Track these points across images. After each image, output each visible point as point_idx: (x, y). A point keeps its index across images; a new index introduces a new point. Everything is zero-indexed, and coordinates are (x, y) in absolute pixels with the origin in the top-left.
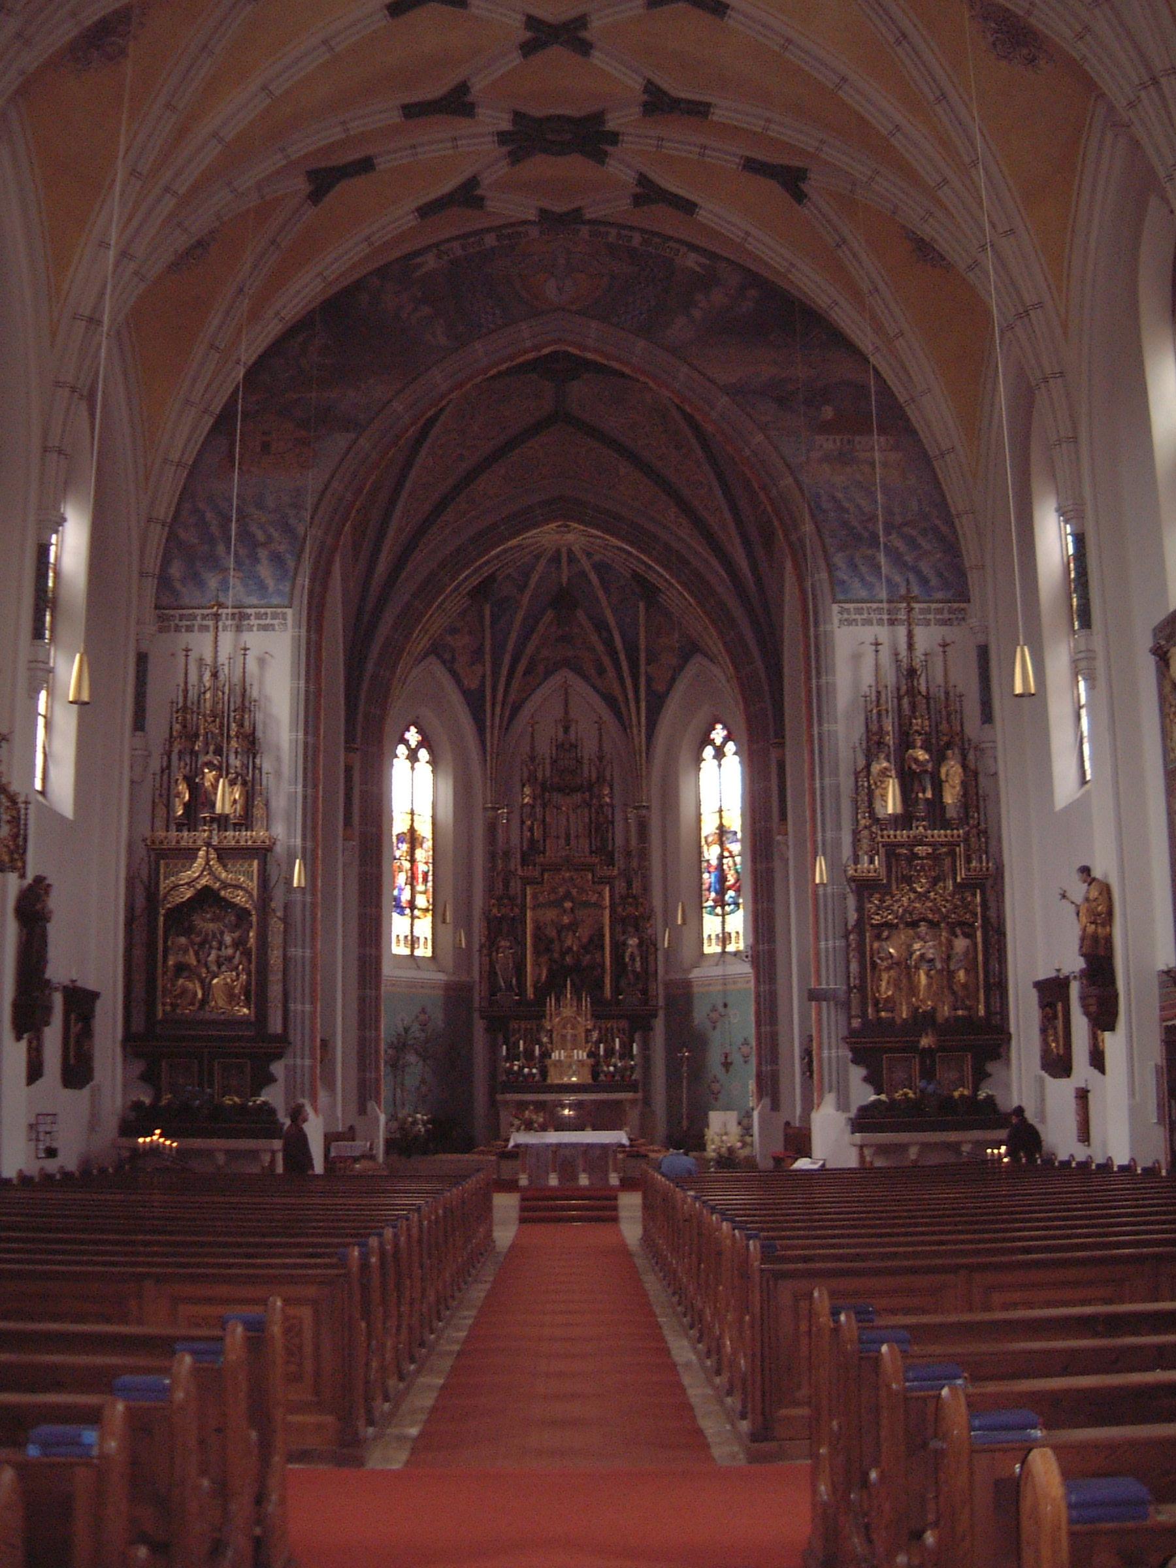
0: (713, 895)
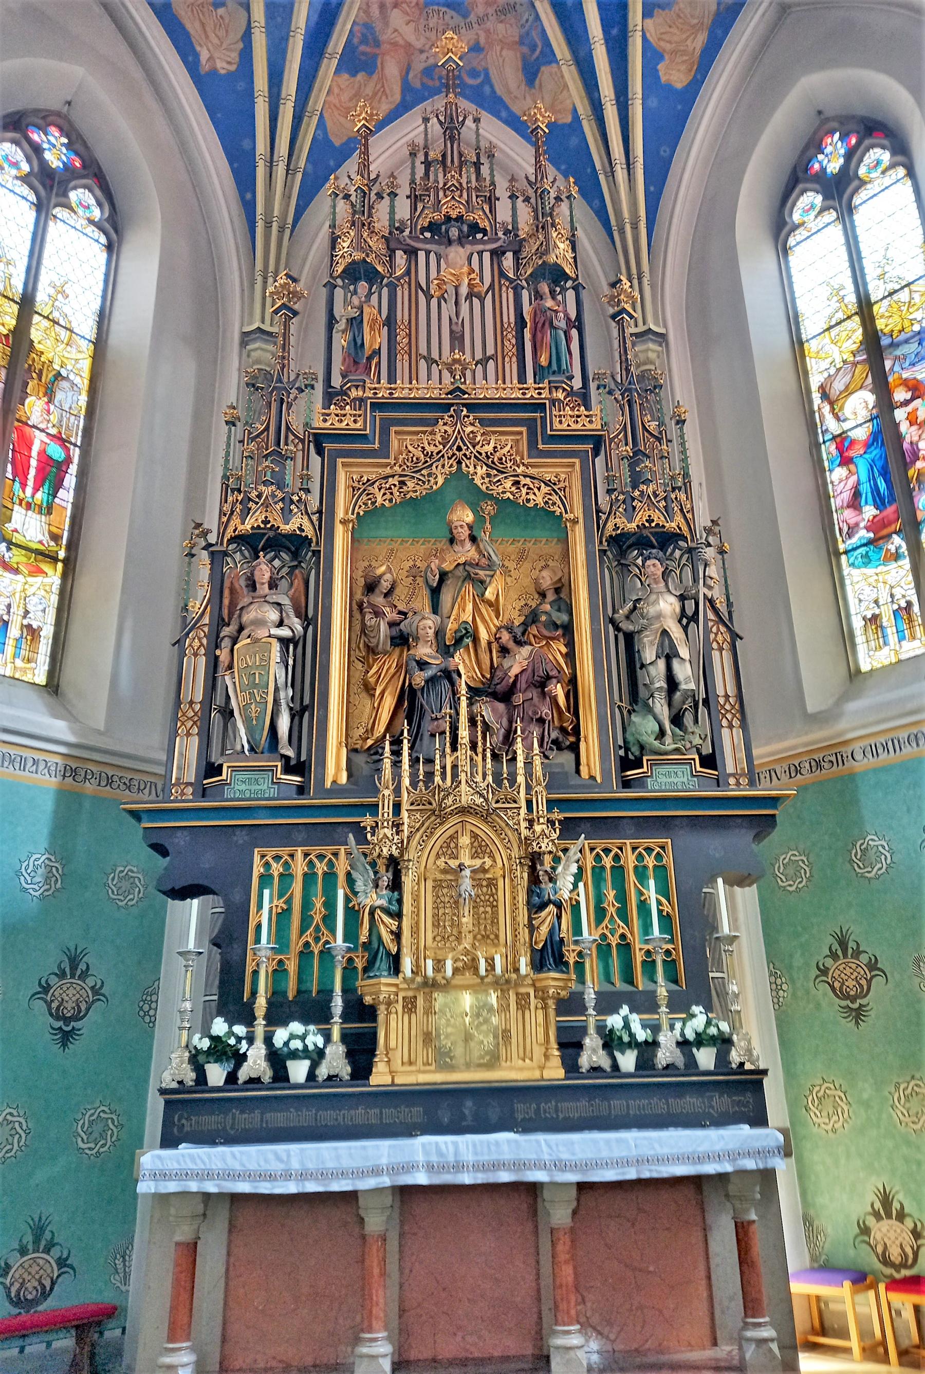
0: (869, 511)
